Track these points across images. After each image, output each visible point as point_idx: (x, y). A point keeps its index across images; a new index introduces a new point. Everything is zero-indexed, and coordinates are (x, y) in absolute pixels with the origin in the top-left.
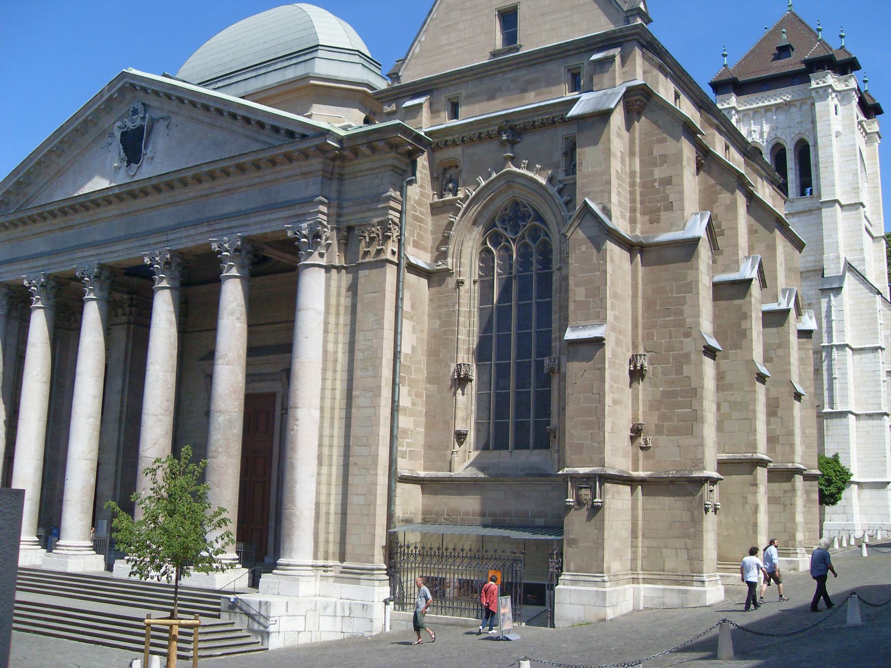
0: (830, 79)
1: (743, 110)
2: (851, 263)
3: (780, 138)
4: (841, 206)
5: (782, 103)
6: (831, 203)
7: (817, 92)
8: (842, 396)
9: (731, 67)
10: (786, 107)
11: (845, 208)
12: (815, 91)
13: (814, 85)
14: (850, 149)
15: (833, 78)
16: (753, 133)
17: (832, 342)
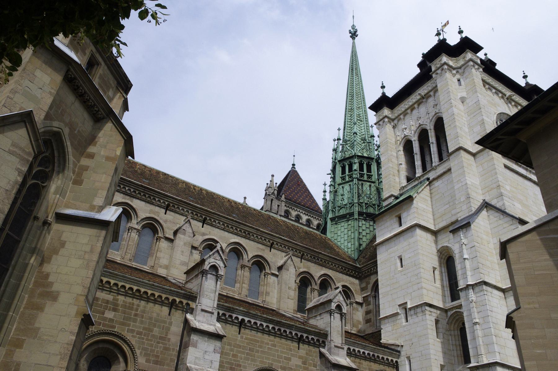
0: (444, 59)
1: (397, 117)
2: (490, 203)
3: (422, 125)
4: (474, 155)
5: (420, 99)
6: (457, 153)
7: (437, 74)
8: (487, 345)
9: (390, 93)
10: (424, 100)
11: (478, 156)
12: (434, 74)
13: (433, 69)
14: (475, 105)
15: (452, 60)
16: (404, 130)
17: (468, 282)
